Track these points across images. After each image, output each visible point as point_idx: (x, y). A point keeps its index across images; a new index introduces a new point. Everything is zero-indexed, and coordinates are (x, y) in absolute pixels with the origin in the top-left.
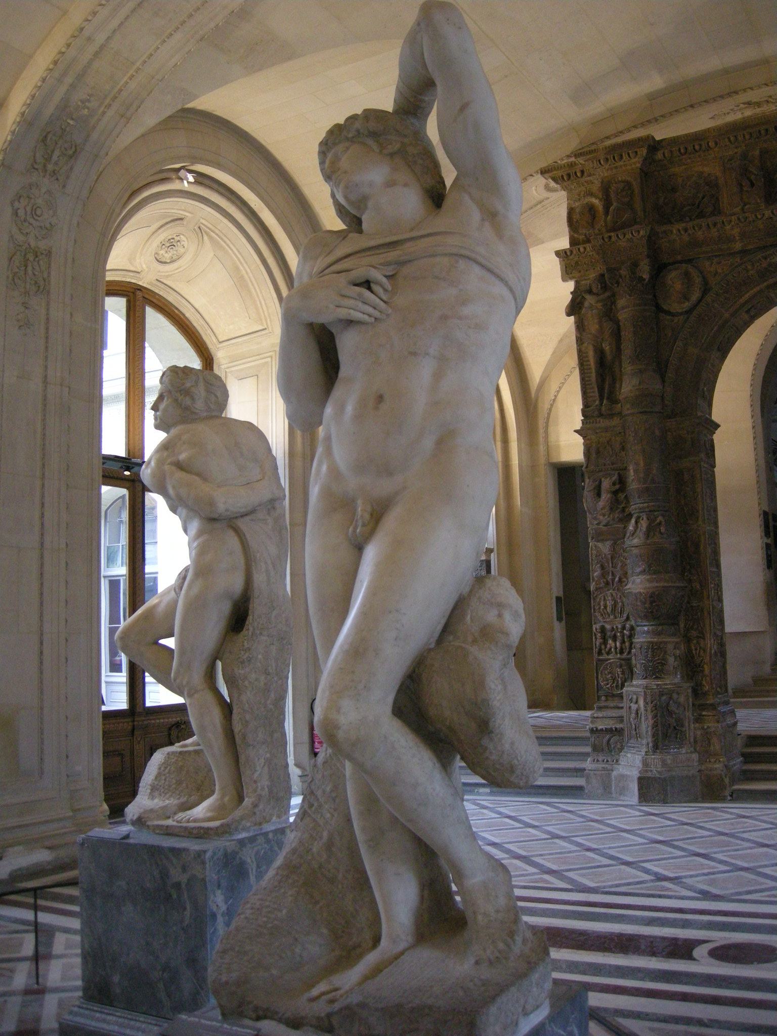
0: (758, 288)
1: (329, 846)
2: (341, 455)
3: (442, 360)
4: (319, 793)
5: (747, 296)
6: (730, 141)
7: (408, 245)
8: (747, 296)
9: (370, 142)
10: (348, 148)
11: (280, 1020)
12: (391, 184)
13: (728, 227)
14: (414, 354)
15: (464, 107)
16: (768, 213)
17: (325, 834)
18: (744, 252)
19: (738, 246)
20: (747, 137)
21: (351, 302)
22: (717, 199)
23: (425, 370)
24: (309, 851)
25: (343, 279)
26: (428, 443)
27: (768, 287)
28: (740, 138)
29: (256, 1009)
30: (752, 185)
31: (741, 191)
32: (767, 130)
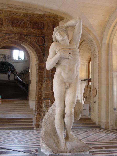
0: (7, 41)
1: (50, 130)
2: (64, 76)
3: (77, 66)
4: (47, 123)
5: (5, 41)
6: (7, 13)
7: (71, 49)
8: (5, 41)
9: (64, 31)
10: (61, 32)
11: (64, 153)
12: (67, 39)
13: (4, 28)
14: (75, 65)
15: (79, 33)
16: (11, 28)
17: (49, 129)
18: (6, 34)
19: (5, 32)
20: (10, 13)
21: (70, 56)
22: (2, 23)
23: (76, 66)
24: (47, 131)
25: (68, 52)
26: (76, 76)
27: (9, 41)
28: (9, 13)
29: (60, 152)
30: (9, 22)
31: (7, 23)
32: (14, 14)
